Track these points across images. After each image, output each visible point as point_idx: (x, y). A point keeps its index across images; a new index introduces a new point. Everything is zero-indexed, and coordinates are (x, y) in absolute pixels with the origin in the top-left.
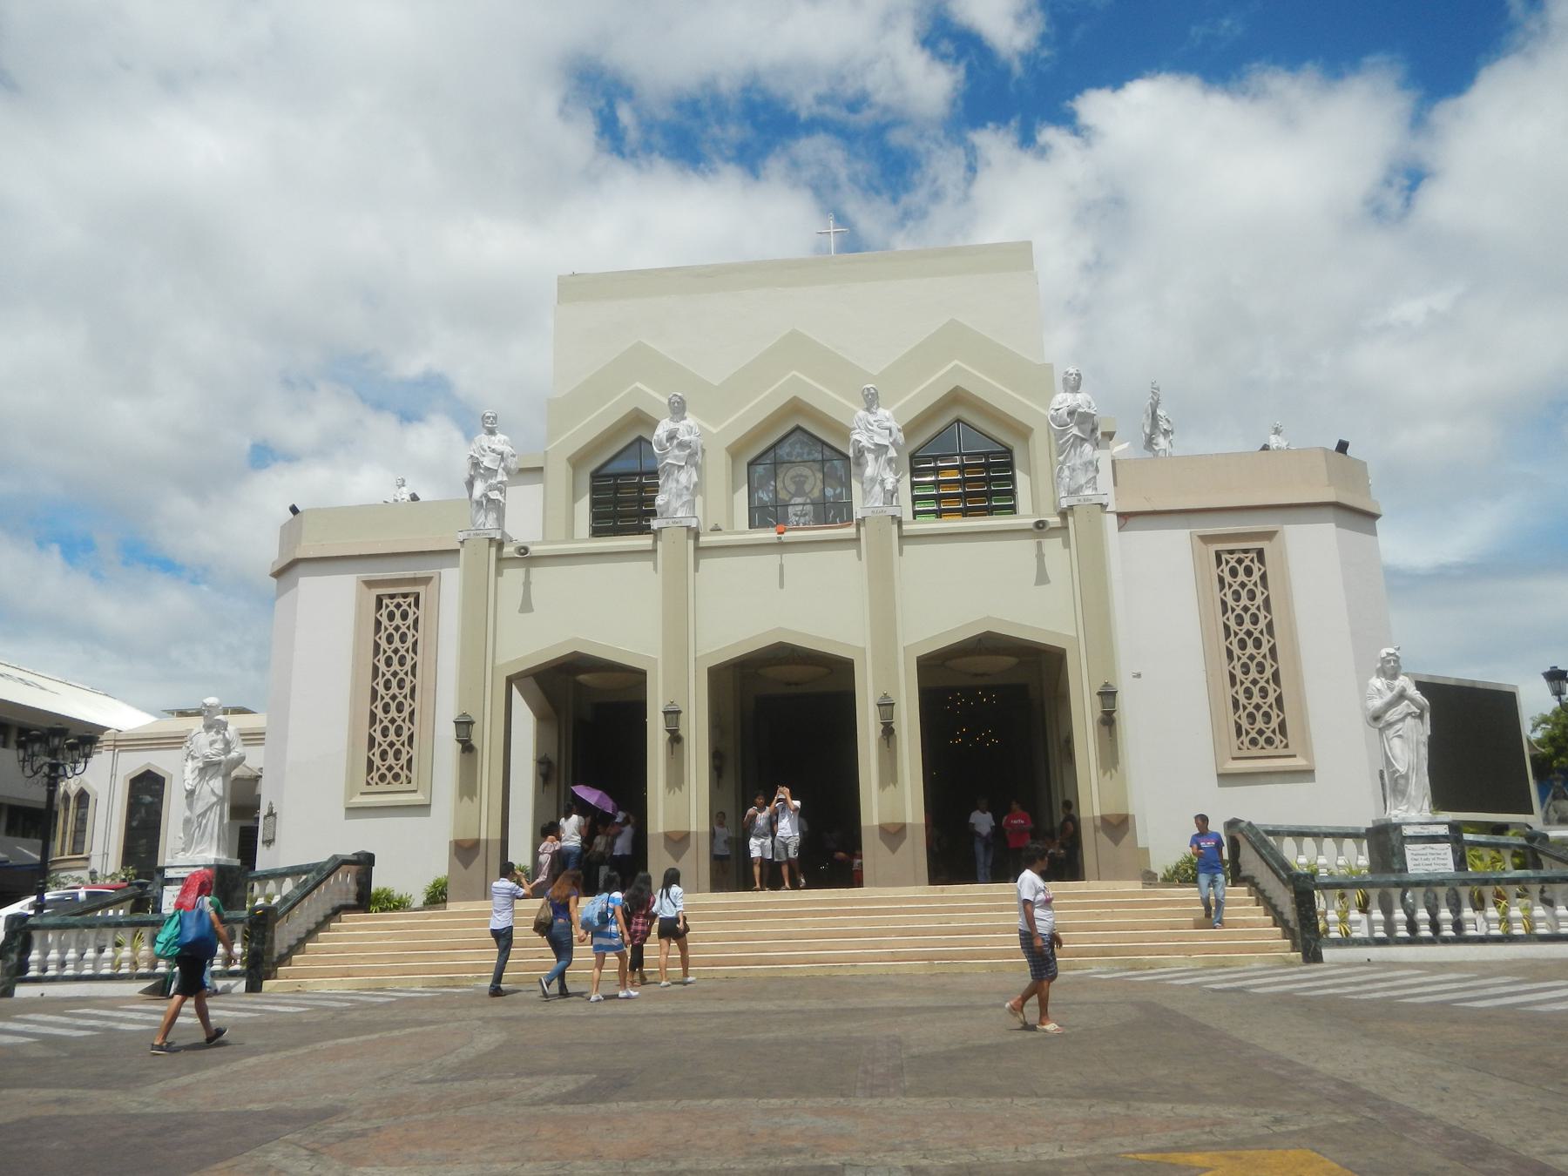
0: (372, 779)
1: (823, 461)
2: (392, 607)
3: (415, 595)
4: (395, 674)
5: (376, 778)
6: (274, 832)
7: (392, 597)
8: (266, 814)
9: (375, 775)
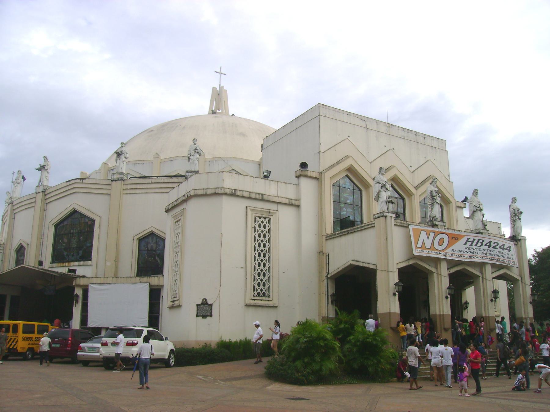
0: (255, 294)
1: (397, 198)
2: (260, 222)
3: (269, 219)
4: (262, 251)
5: (256, 294)
6: (211, 312)
7: (260, 218)
8: (200, 303)
9: (256, 293)
